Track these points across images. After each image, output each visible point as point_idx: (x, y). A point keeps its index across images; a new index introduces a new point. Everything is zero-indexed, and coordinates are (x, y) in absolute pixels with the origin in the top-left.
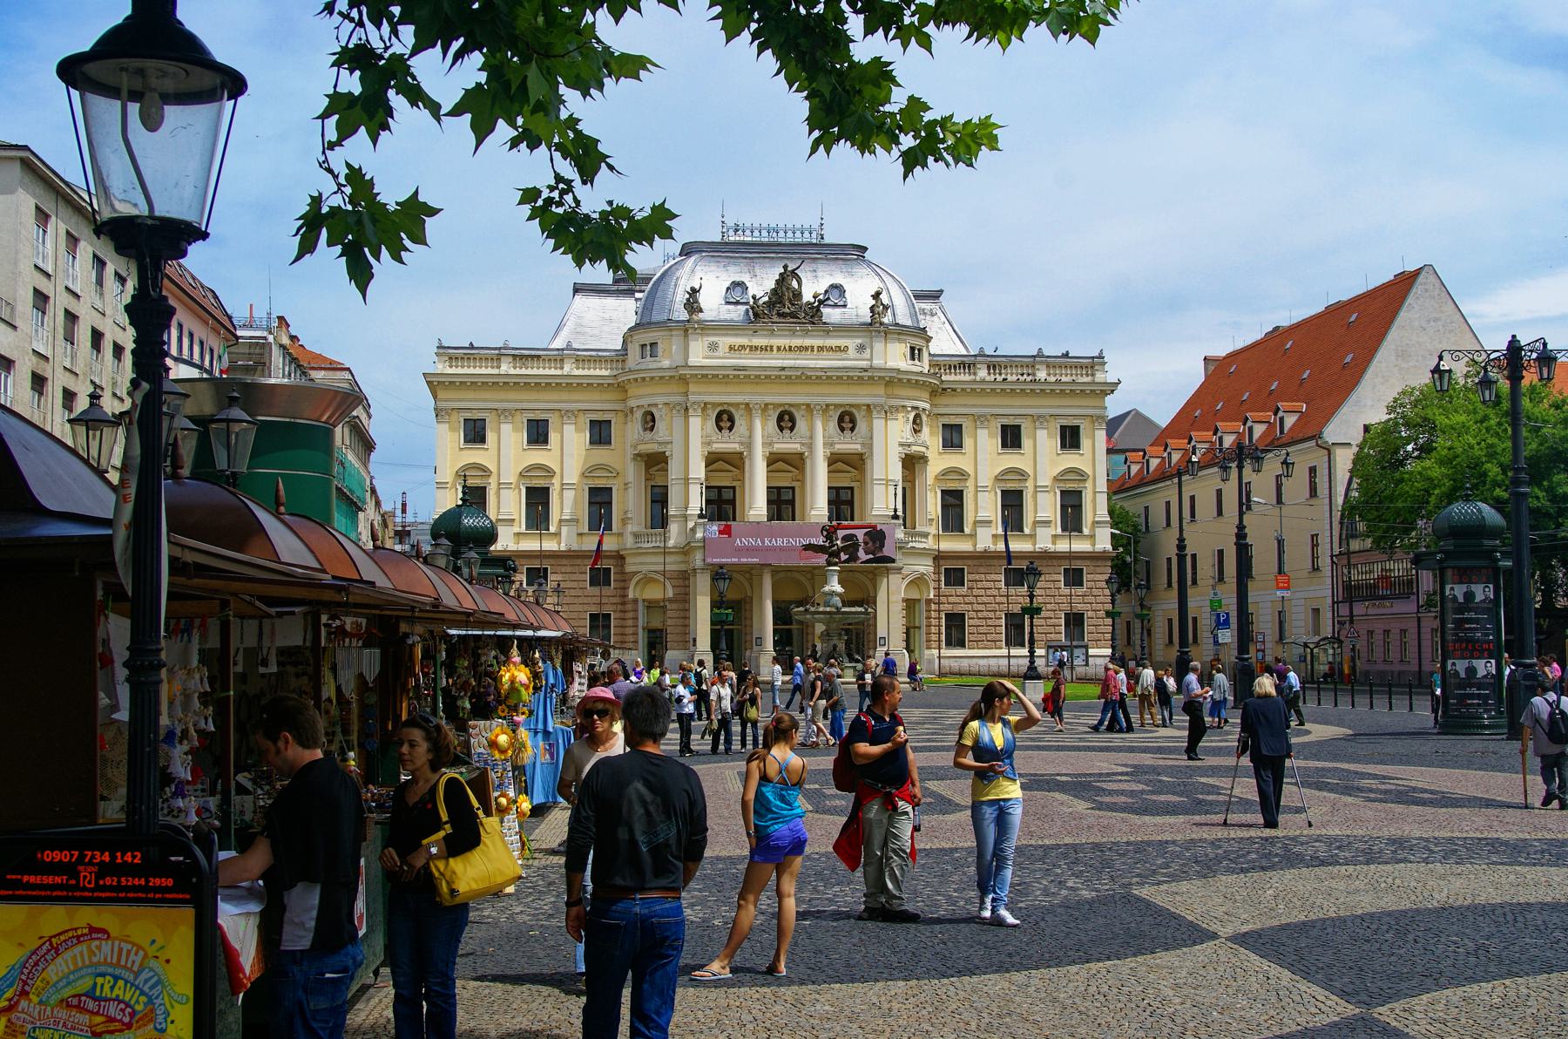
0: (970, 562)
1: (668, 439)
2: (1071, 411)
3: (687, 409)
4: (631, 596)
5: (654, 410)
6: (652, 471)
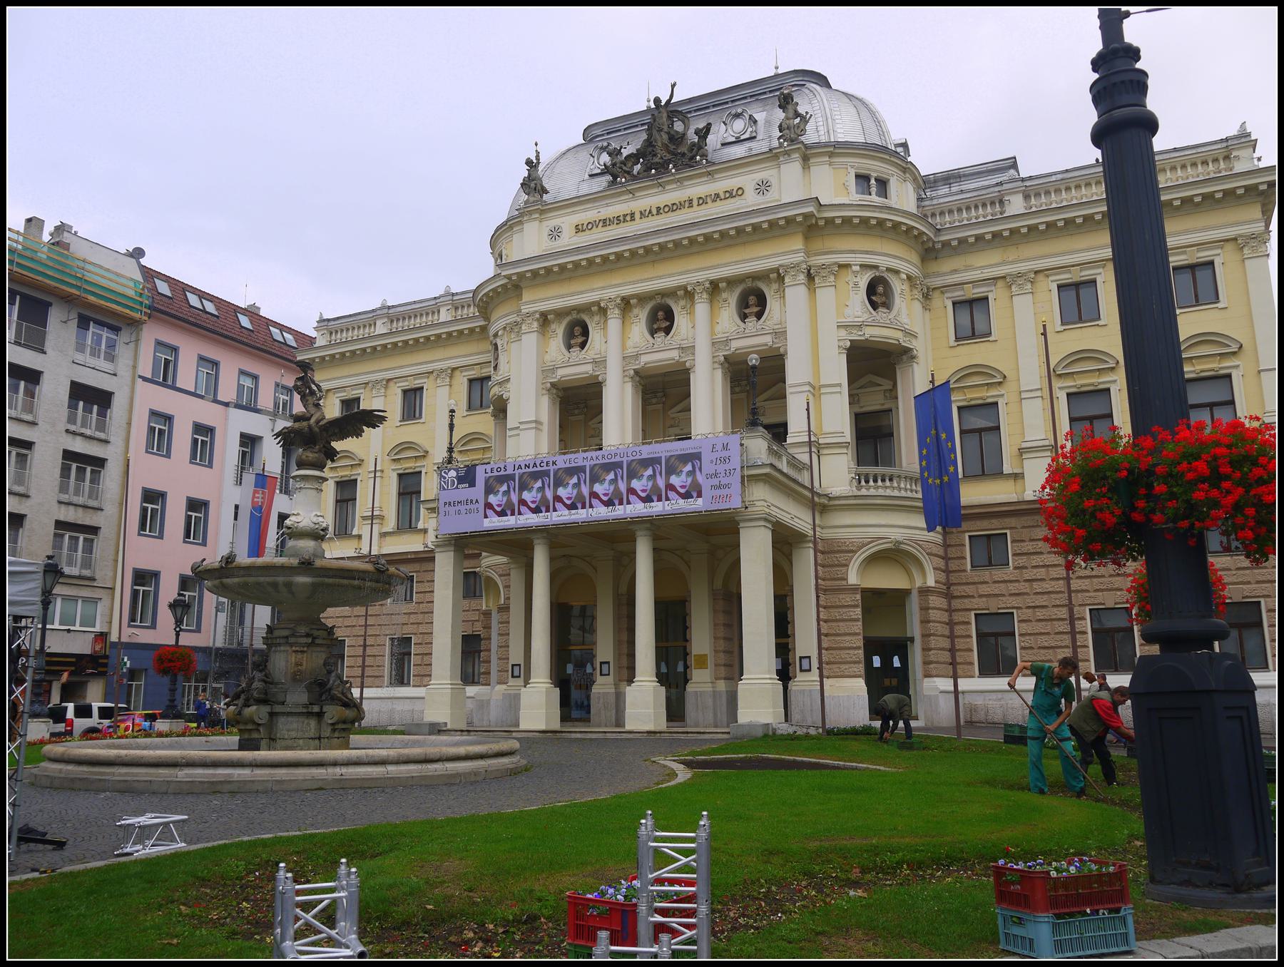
0: (1012, 521)
5: (499, 342)
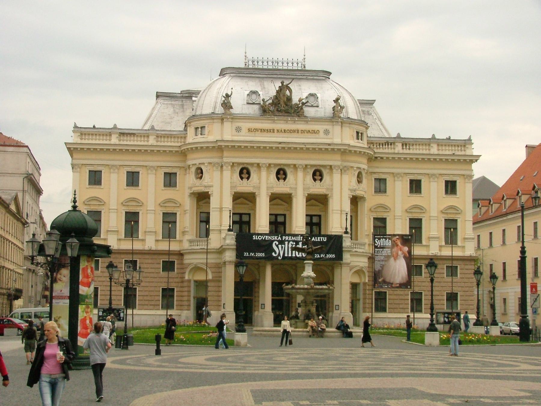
1: (210, 184)
2: (452, 172)
3: (222, 167)
4: (187, 278)
6: (201, 203)
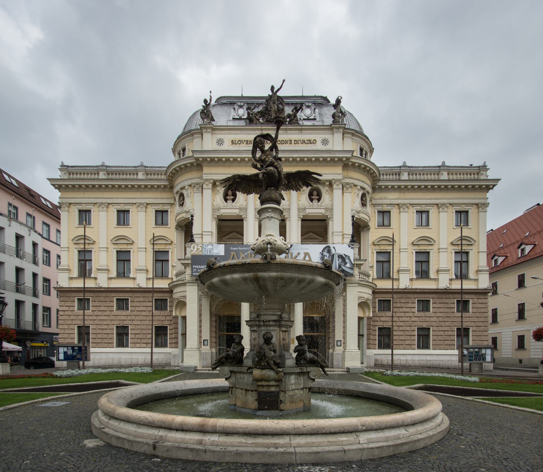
5: (184, 192)
